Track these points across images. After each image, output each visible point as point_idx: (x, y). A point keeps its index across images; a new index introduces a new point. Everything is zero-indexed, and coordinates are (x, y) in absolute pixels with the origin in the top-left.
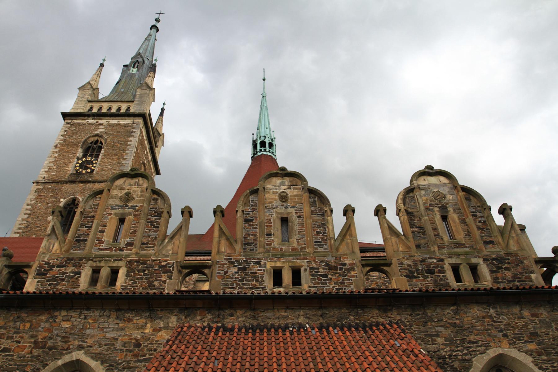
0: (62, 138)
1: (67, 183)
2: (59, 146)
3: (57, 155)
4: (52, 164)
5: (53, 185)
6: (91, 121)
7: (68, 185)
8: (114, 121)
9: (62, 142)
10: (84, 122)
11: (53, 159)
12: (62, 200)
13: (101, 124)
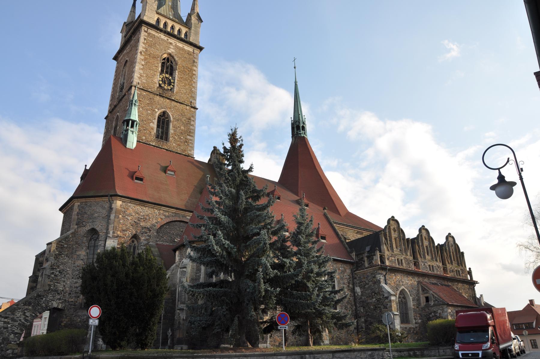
0: (144, 46)
1: (157, 95)
2: (143, 53)
3: (143, 63)
4: (141, 72)
5: (147, 93)
6: (162, 36)
7: (158, 97)
8: (180, 45)
9: (144, 50)
10: (156, 34)
12: (157, 110)
13: (171, 43)
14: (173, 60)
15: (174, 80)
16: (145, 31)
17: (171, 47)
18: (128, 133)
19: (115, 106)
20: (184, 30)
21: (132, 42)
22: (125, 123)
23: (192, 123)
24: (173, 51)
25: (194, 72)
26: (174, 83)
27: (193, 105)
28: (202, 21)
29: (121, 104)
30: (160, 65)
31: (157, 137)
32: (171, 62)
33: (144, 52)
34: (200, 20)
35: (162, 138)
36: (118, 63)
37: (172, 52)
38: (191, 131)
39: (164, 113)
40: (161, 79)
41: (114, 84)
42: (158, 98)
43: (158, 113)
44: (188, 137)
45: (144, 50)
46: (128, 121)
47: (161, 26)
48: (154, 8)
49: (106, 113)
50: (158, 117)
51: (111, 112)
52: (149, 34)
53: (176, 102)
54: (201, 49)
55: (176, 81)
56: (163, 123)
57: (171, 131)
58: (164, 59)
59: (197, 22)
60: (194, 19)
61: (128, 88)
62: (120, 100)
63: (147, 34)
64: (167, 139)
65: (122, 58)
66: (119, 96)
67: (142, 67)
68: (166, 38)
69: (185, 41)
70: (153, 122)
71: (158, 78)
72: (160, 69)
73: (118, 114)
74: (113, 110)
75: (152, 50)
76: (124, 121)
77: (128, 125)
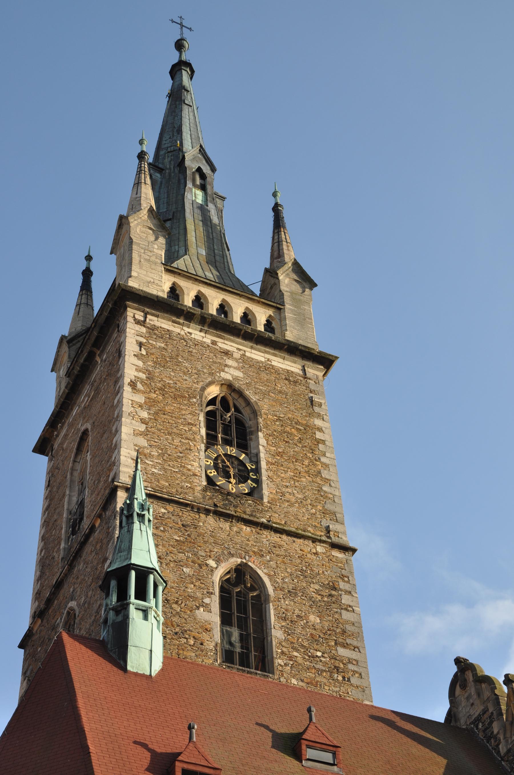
0: (140, 363)
1: (207, 512)
2: (139, 386)
3: (145, 414)
4: (143, 442)
5: (171, 508)
6: (196, 333)
7: (211, 519)
8: (258, 355)
9: (143, 376)
10: (176, 329)
11: (142, 428)
12: (212, 563)
13: (227, 353)
14: (241, 403)
15: (257, 463)
16: (138, 322)
17: (230, 362)
18: (127, 617)
19: (59, 585)
20: (261, 315)
21: (98, 371)
22: (113, 583)
23: (346, 600)
24: (239, 374)
25: (319, 435)
26: (257, 471)
27: (335, 540)
28: (312, 285)
29: (80, 566)
30: (202, 418)
31: (228, 657)
32: (237, 410)
33: (142, 382)
34: (306, 280)
35: (244, 662)
36: (50, 460)
37: (236, 378)
38: (349, 628)
39: (241, 572)
40: (211, 462)
41: (47, 509)
42: (210, 522)
43: (219, 573)
44: (342, 651)
45: (143, 376)
46: (121, 575)
47: (188, 301)
48: (157, 256)
49: (23, 624)
50: (222, 589)
51: (39, 615)
52: (153, 329)
53: (277, 531)
54: (326, 361)
55: (263, 464)
56: (242, 607)
57: (277, 634)
58: (212, 402)
59: (297, 288)
60: (286, 280)
61: (97, 509)
62: (74, 557)
63: (144, 330)
64: (265, 664)
65: (66, 435)
66: (68, 550)
67: (142, 428)
68: (208, 339)
69: (269, 339)
70: (207, 608)
71: (200, 461)
72: (203, 431)
73: (73, 604)
74: (49, 602)
75: (168, 376)
76: (109, 575)
77: (123, 595)
